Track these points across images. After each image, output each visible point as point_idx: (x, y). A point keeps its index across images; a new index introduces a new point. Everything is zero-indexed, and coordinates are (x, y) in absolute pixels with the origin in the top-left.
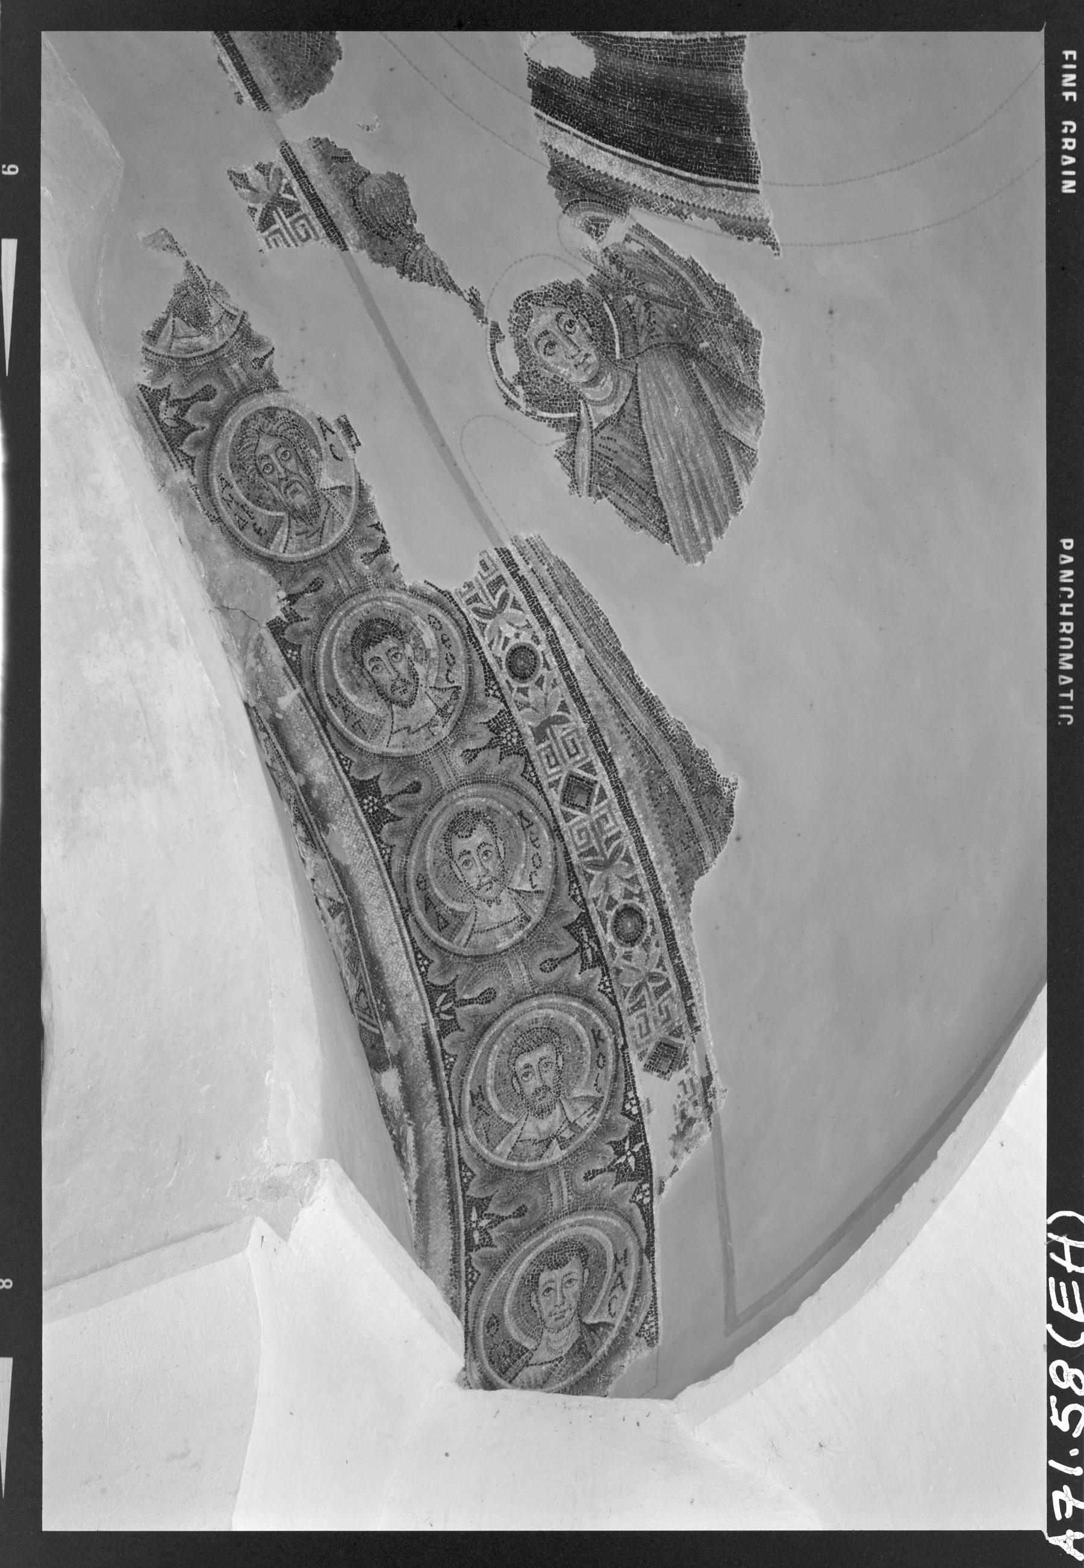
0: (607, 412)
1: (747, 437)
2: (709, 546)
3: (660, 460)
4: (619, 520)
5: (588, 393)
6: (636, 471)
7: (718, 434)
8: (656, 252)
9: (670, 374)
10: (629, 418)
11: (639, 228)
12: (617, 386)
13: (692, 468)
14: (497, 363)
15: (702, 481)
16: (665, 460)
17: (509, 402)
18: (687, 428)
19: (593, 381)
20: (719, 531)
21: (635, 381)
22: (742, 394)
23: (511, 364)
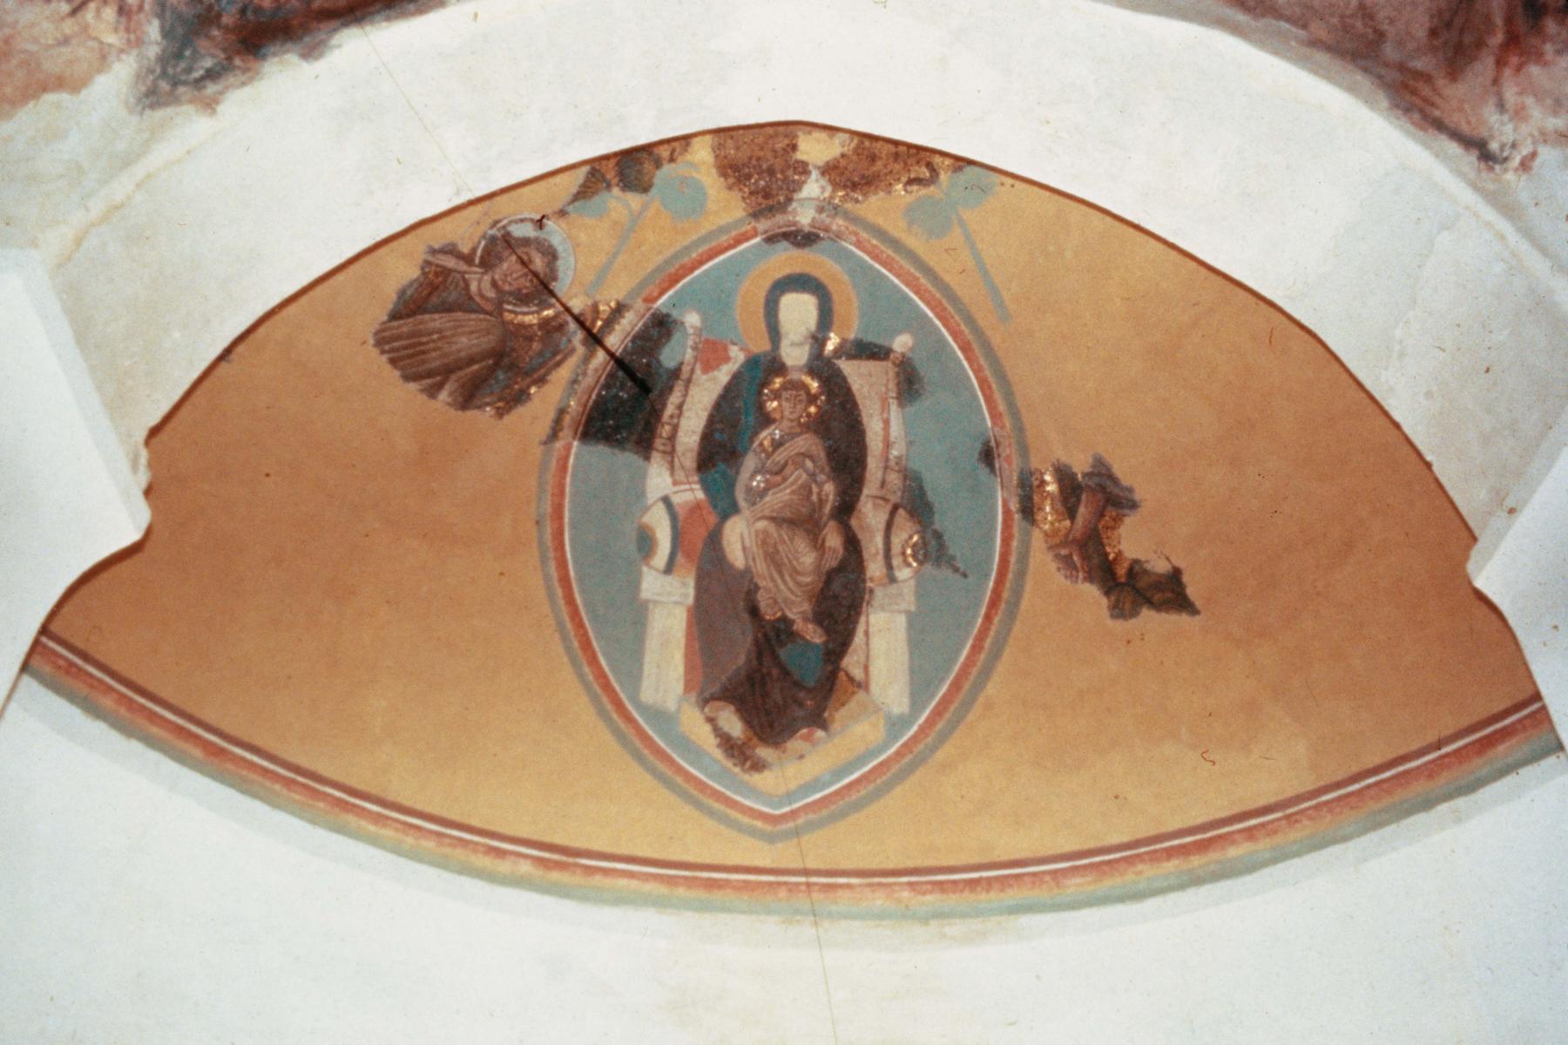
0: (474, 287)
1: (444, 395)
2: (383, 352)
3: (436, 321)
4: (405, 282)
5: (487, 278)
6: (435, 300)
7: (447, 371)
8: (558, 358)
9: (486, 342)
10: (467, 304)
11: (573, 350)
12: (487, 299)
13: (432, 345)
14: (522, 221)
15: (424, 352)
16: (437, 325)
17: (497, 222)
18: (454, 348)
19: (494, 284)
20: (393, 362)
21: (487, 313)
22: (468, 398)
23: (519, 231)
